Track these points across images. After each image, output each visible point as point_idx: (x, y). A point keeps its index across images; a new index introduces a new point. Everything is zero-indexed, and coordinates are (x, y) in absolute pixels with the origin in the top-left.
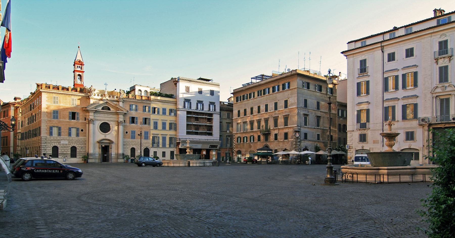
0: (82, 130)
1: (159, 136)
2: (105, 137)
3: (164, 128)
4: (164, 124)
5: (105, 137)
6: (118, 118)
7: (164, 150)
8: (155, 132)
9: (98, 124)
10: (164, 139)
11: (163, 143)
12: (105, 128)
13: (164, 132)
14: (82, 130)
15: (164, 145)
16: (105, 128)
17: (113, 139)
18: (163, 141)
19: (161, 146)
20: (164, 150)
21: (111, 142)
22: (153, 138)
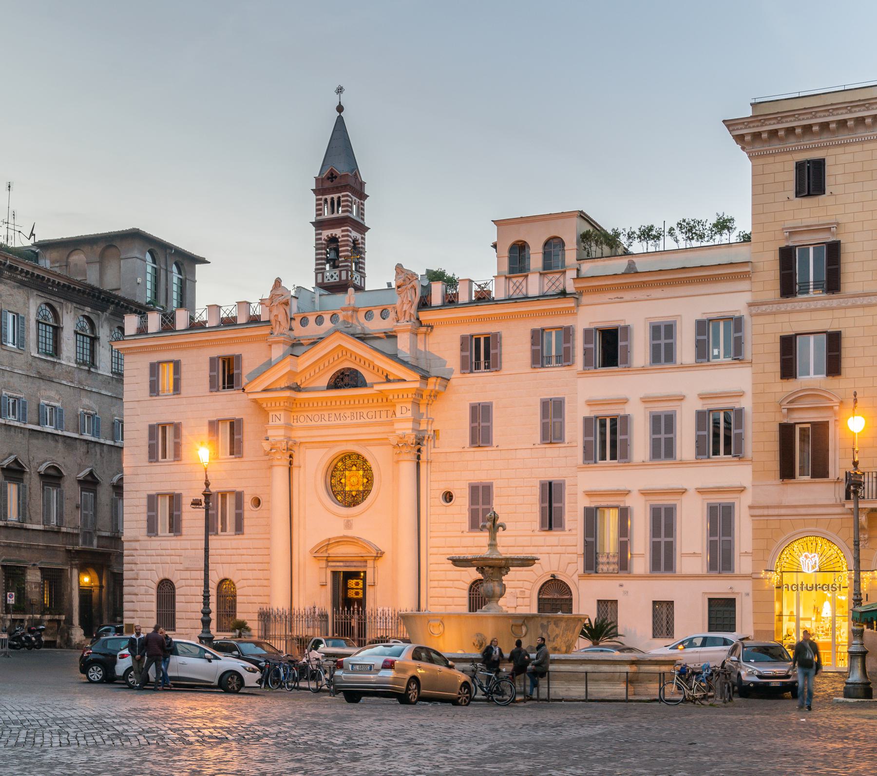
0: (257, 502)
1: (628, 502)
2: (348, 525)
3: (663, 448)
4: (663, 425)
5: (348, 525)
6: (392, 423)
7: (663, 589)
8: (607, 477)
9: (313, 465)
10: (663, 521)
11: (655, 548)
12: (348, 480)
13: (664, 477)
14: (257, 502)
15: (663, 559)
16: (348, 480)
17: (378, 539)
18: (655, 531)
19: (641, 563)
20: (663, 589)
21: (379, 555)
22: (591, 516)
